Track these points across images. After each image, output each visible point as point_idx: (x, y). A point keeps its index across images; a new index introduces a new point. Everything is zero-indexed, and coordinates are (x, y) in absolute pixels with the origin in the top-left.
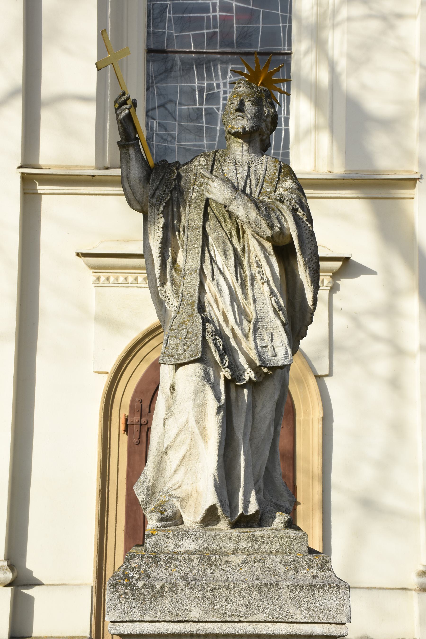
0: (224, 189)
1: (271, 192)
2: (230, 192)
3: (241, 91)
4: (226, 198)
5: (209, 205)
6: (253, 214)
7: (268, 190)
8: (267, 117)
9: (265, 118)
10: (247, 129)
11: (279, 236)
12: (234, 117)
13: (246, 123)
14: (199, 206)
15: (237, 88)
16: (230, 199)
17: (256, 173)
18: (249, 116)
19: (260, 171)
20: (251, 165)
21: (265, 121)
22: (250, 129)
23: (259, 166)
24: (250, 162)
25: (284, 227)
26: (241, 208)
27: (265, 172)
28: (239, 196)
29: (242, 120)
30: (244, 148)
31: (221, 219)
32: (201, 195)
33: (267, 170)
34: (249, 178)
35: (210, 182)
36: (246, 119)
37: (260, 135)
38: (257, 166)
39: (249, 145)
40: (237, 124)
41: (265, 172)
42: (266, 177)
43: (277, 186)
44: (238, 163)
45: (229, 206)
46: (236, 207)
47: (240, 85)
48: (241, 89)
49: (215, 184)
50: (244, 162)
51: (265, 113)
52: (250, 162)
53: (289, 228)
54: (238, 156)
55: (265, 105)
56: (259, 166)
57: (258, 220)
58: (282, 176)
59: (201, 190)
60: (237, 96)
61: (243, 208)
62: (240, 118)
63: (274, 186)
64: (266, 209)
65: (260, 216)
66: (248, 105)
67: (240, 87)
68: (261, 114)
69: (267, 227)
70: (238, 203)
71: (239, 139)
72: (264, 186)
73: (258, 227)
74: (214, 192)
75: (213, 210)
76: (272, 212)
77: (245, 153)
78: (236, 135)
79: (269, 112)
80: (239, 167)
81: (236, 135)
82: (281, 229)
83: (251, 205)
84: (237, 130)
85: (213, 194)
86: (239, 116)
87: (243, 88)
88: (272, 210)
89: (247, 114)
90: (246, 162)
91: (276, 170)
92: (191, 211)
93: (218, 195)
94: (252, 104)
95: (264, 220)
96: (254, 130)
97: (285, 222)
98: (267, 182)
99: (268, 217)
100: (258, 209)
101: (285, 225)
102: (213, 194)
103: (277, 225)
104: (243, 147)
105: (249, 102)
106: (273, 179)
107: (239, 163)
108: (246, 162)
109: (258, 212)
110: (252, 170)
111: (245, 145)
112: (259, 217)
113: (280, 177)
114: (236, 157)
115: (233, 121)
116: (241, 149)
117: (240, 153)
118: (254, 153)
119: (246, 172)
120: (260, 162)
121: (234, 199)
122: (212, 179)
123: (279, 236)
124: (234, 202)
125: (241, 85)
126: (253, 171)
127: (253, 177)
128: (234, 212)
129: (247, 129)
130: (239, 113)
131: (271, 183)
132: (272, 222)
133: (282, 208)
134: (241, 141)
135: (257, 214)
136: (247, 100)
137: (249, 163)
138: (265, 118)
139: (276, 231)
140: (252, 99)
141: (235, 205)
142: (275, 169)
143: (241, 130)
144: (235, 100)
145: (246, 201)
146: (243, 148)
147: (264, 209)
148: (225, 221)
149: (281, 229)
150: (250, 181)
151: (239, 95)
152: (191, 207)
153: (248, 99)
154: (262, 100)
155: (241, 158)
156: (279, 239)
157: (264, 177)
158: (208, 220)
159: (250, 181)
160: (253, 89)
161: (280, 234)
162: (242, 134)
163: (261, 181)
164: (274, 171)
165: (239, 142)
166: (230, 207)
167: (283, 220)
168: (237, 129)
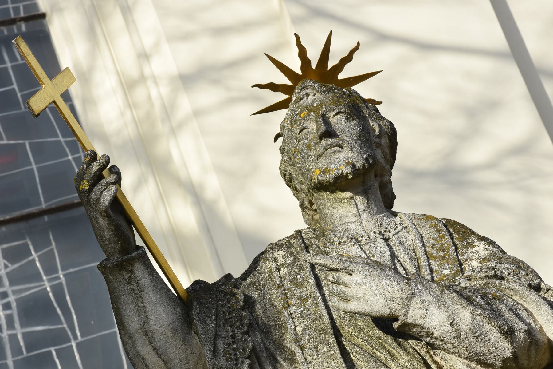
0: (380, 280)
1: (456, 274)
2: (395, 283)
3: (313, 102)
4: (393, 299)
5: (342, 336)
6: (465, 315)
7: (446, 272)
8: (379, 136)
9: (378, 140)
10: (359, 164)
11: (529, 350)
12: (319, 151)
13: (351, 154)
14: (322, 342)
15: (302, 99)
16: (401, 299)
17: (405, 249)
18: (350, 141)
19: (410, 242)
20: (387, 235)
21: (379, 145)
22: (363, 165)
23: (403, 233)
24: (382, 231)
25: (532, 328)
26: (433, 308)
27: (422, 241)
28: (419, 286)
29: (340, 152)
30: (360, 206)
31: (383, 356)
32: (316, 319)
33: (422, 237)
34: (396, 260)
35: (344, 277)
36: (346, 148)
37: (376, 176)
38: (399, 235)
39: (368, 198)
40: (333, 162)
41: (422, 241)
42: (427, 249)
43: (459, 260)
44: (360, 239)
45: (406, 312)
46: (422, 312)
47: (306, 91)
48: (311, 97)
49: (357, 278)
50: (372, 234)
51: (374, 131)
52: (382, 231)
53: (541, 328)
54: (353, 227)
55: (369, 115)
56: (403, 233)
57: (478, 324)
58: (457, 239)
59: (311, 311)
60: (310, 111)
61: (439, 307)
62: (335, 149)
63: (454, 260)
64: (482, 298)
65: (481, 315)
66: (338, 121)
67: (308, 95)
68: (368, 132)
69: (499, 335)
70: (423, 301)
71: (343, 191)
72: (434, 268)
73: (481, 342)
74: (361, 295)
75: (354, 342)
76: (498, 302)
77: (364, 217)
78: (338, 184)
79: (380, 127)
80: (366, 244)
81: (338, 184)
82: (529, 332)
83: (451, 297)
84: (340, 172)
85: (358, 299)
86: (332, 145)
87: (315, 95)
88: (494, 298)
89: (346, 138)
90: (374, 232)
91: (439, 231)
92: (309, 359)
93: (371, 298)
94: (347, 118)
95: (490, 322)
96: (370, 164)
97: (530, 317)
98: (435, 258)
99: (495, 314)
100: (469, 300)
101: (533, 324)
102: (358, 299)
103: (520, 326)
104: (356, 204)
105: (339, 116)
106: (443, 250)
107: (362, 237)
108: (374, 232)
109: (473, 308)
110: (394, 242)
111: (360, 201)
112: (479, 318)
113: (457, 242)
114: (349, 230)
115: (321, 159)
116: (354, 211)
117: (355, 220)
118: (381, 213)
119: (386, 249)
120: (400, 227)
121: (414, 295)
122: (346, 268)
123: (529, 350)
124: (414, 300)
125: (309, 90)
126: (397, 244)
127: (402, 255)
128: (421, 322)
129: (359, 164)
130: (330, 141)
131: (444, 257)
132: (508, 321)
133: (512, 289)
134: (348, 194)
135: (473, 313)
136: (333, 113)
137: (380, 233)
138: (378, 140)
139: (522, 340)
140: (343, 108)
141: (419, 306)
142: (437, 231)
143: (348, 169)
144: (306, 120)
145: (438, 292)
146: (357, 208)
147: (479, 299)
148: (393, 357)
149: (529, 332)
150: (402, 265)
151: (310, 109)
152: (306, 350)
153: (336, 111)
154: (359, 107)
155: (360, 227)
156: (529, 359)
157: (425, 251)
158: (354, 365)
159: (402, 265)
160: (334, 92)
161: (531, 344)
162: (350, 176)
163: (423, 260)
164: (437, 234)
165: (345, 199)
166: (410, 314)
167: (524, 314)
168: (338, 169)
